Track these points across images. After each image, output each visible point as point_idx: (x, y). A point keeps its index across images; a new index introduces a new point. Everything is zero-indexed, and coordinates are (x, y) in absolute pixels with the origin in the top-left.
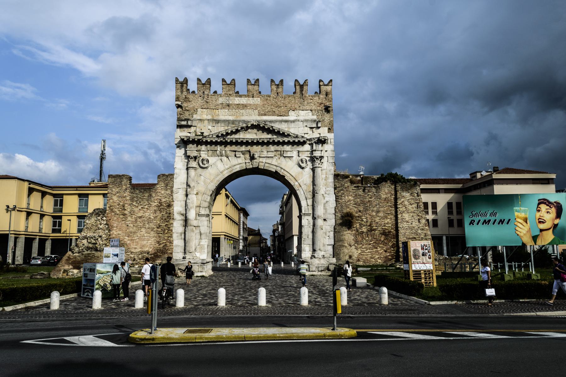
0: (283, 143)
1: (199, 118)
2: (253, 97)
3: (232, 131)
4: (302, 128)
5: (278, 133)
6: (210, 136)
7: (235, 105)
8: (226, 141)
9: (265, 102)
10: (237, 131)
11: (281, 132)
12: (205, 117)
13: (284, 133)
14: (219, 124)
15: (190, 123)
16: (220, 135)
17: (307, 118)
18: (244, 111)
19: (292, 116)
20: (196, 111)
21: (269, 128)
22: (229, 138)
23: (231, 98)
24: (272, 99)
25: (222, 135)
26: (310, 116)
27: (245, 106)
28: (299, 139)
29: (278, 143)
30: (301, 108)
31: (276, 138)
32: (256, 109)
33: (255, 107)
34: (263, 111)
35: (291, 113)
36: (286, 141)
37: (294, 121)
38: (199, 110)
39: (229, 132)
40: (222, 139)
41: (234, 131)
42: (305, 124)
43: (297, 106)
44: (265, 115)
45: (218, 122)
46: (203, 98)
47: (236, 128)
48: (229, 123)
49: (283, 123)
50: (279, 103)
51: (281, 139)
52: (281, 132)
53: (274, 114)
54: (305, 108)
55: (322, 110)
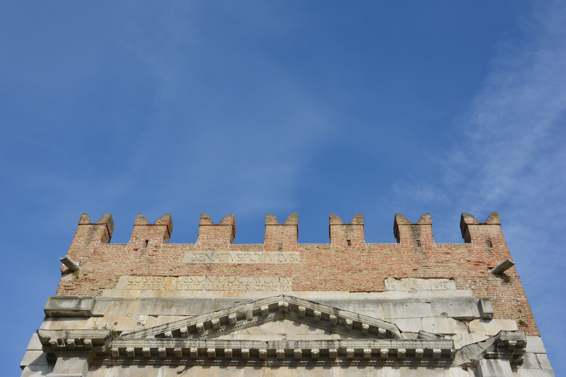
0: (378, 360)
1: (117, 295)
2: (280, 249)
3: (208, 325)
4: (433, 320)
5: (356, 330)
6: (137, 336)
7: (228, 266)
8: (186, 352)
9: (315, 260)
10: (227, 324)
11: (366, 326)
12: (136, 293)
13: (373, 333)
14: (174, 310)
15: (85, 306)
16: (169, 333)
17: (441, 295)
18: (251, 279)
19: (396, 291)
20: (113, 281)
21: (325, 317)
22: (193, 345)
23: (219, 252)
24: (333, 253)
25: (177, 334)
26: (451, 290)
27: (255, 270)
28: (427, 345)
29: (360, 359)
30: (421, 273)
31: (352, 345)
32: (288, 274)
33: (287, 271)
34: (308, 279)
35: (390, 283)
36: (385, 351)
37: (403, 302)
38: (124, 280)
39: (200, 325)
40: (172, 344)
41: (214, 321)
42: (440, 309)
43: (406, 268)
44: (314, 289)
45: (169, 303)
46: (143, 253)
47: (222, 314)
48: (203, 306)
49: (371, 307)
50: (354, 262)
51: (367, 346)
52: (366, 326)
53: (340, 286)
54: (429, 273)
55: (486, 278)
